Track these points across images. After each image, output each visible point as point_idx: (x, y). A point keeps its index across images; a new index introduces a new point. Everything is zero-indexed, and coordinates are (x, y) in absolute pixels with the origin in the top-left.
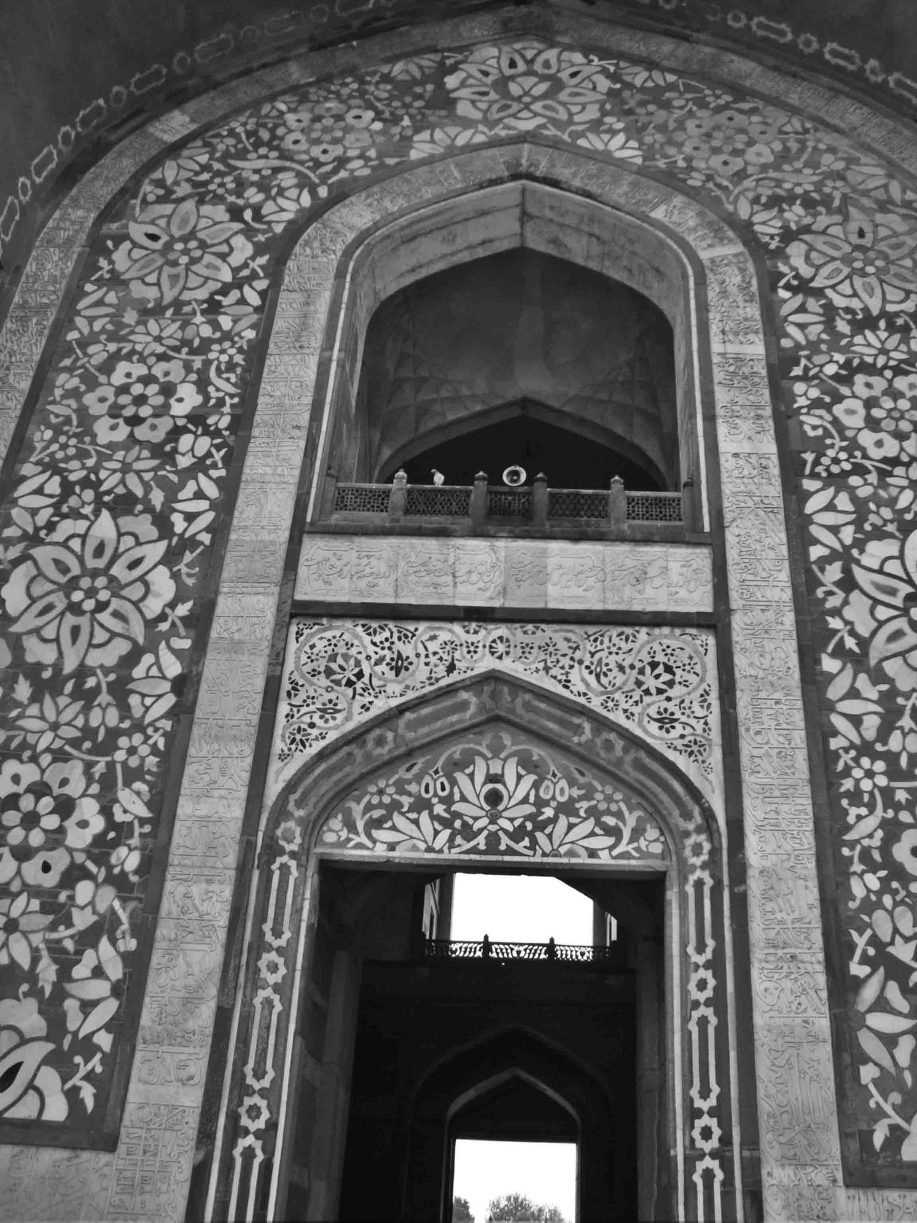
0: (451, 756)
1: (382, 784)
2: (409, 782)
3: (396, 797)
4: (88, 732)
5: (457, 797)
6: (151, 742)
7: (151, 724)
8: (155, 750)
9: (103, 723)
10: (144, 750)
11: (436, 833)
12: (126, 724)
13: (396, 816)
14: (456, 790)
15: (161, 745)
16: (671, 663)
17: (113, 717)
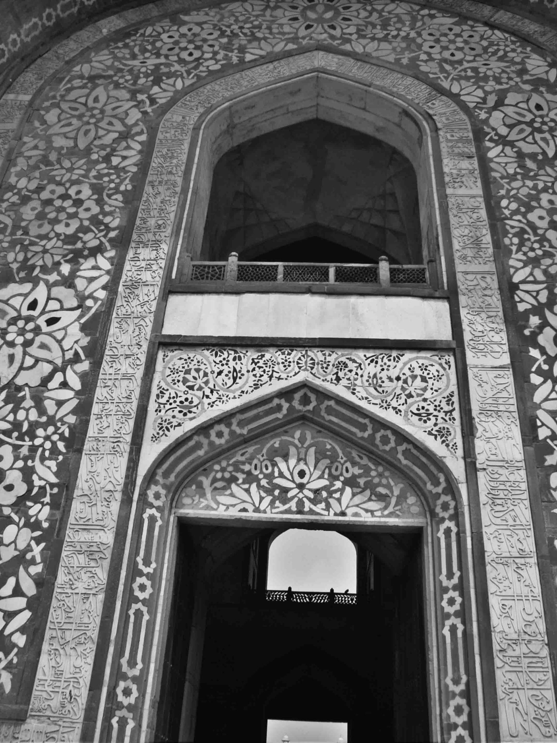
0: (272, 446)
1: (224, 464)
2: (243, 463)
3: (233, 473)
4: (17, 425)
5: (276, 474)
6: (60, 431)
7: (61, 420)
8: (62, 437)
9: (27, 418)
10: (55, 438)
11: (262, 499)
12: (44, 419)
13: (233, 486)
14: (276, 470)
15: (67, 434)
16: (425, 374)
17: (33, 415)
